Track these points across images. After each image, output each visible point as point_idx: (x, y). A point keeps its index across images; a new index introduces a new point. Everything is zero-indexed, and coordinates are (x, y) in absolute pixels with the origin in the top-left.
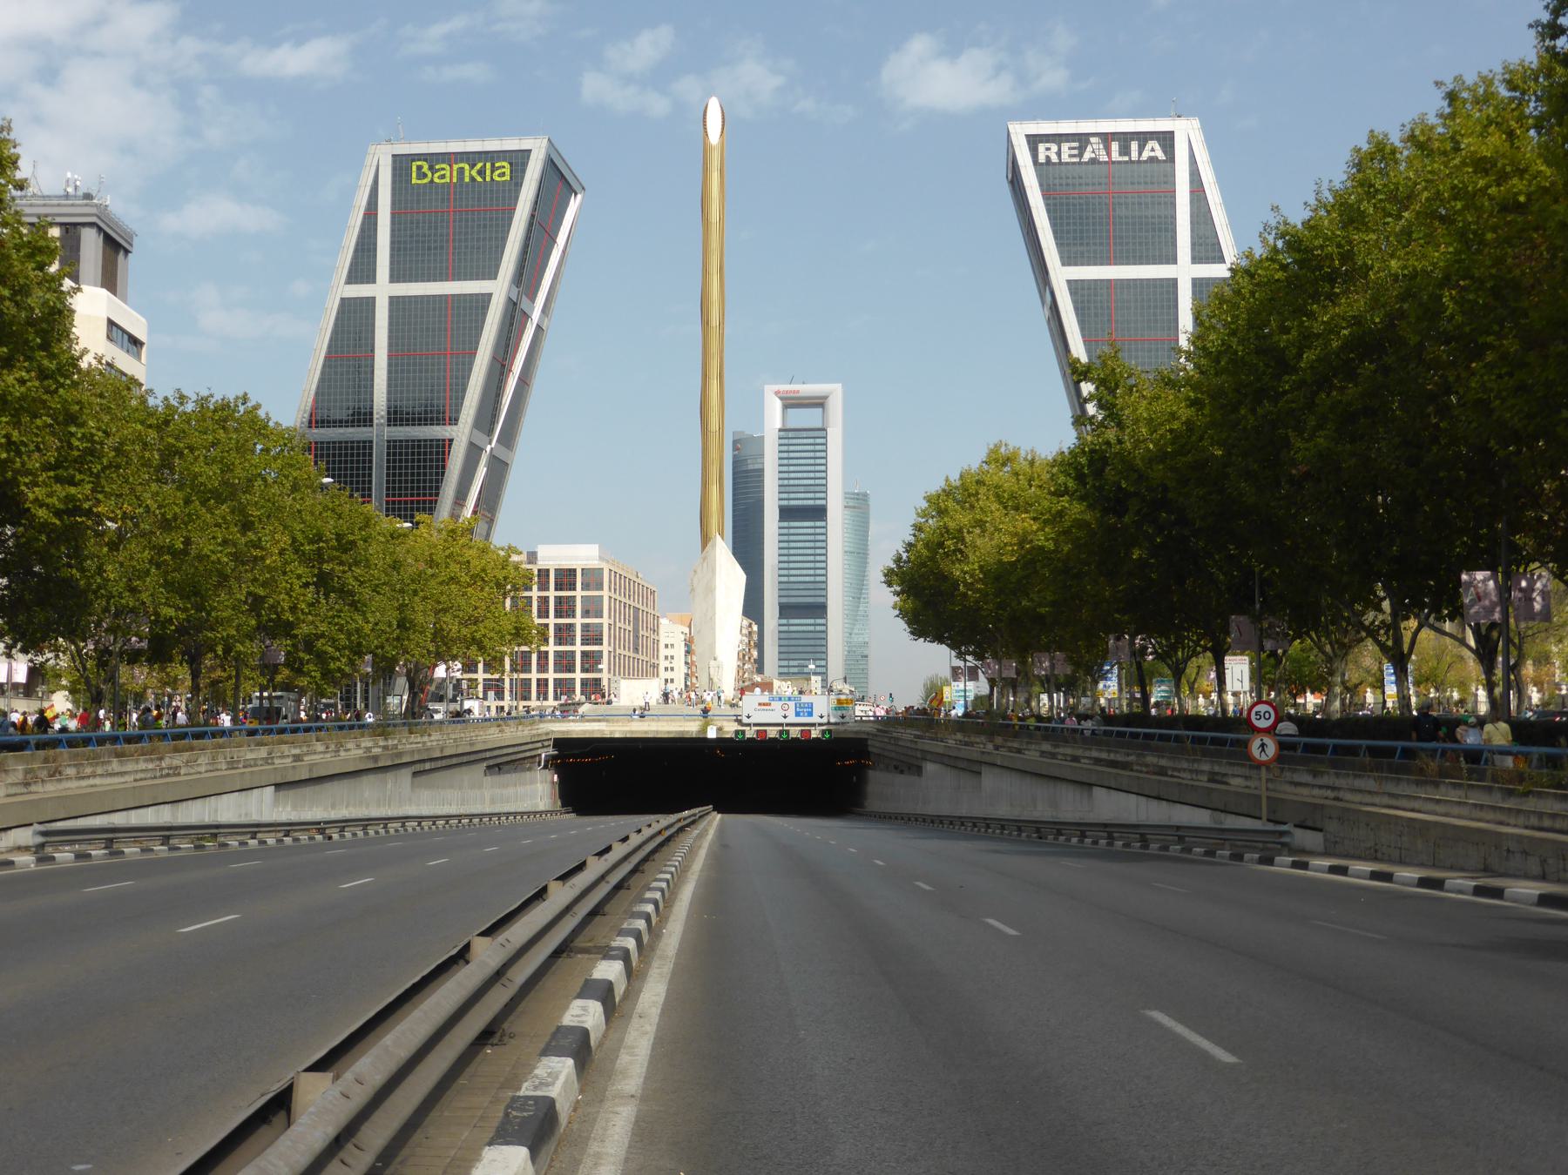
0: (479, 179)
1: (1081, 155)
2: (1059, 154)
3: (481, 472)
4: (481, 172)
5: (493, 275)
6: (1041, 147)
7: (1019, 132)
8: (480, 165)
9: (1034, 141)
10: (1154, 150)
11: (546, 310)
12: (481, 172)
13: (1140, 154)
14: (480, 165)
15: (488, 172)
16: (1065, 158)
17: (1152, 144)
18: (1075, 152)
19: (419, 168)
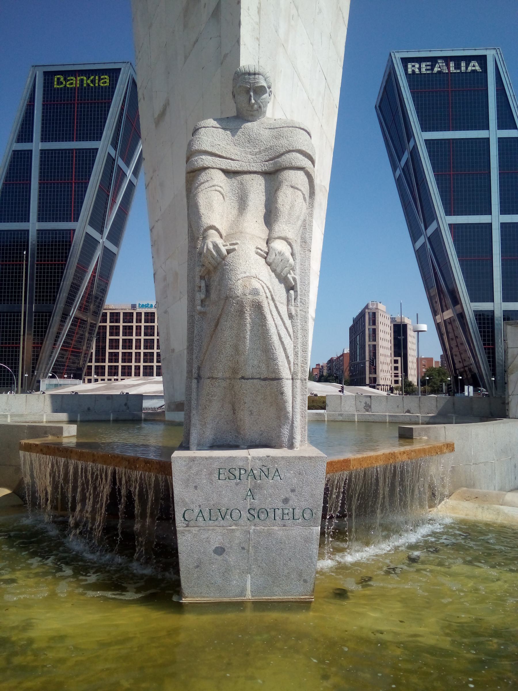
0: (92, 85)
1: (432, 69)
2: (420, 69)
3: (99, 253)
4: (93, 81)
5: (98, 137)
6: (410, 66)
7: (397, 57)
8: (92, 77)
9: (405, 61)
10: (475, 66)
11: (136, 173)
12: (93, 81)
13: (467, 68)
14: (92, 77)
15: (97, 81)
16: (423, 71)
17: (473, 63)
18: (429, 68)
19: (58, 79)
